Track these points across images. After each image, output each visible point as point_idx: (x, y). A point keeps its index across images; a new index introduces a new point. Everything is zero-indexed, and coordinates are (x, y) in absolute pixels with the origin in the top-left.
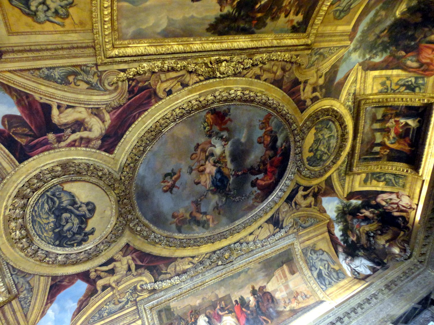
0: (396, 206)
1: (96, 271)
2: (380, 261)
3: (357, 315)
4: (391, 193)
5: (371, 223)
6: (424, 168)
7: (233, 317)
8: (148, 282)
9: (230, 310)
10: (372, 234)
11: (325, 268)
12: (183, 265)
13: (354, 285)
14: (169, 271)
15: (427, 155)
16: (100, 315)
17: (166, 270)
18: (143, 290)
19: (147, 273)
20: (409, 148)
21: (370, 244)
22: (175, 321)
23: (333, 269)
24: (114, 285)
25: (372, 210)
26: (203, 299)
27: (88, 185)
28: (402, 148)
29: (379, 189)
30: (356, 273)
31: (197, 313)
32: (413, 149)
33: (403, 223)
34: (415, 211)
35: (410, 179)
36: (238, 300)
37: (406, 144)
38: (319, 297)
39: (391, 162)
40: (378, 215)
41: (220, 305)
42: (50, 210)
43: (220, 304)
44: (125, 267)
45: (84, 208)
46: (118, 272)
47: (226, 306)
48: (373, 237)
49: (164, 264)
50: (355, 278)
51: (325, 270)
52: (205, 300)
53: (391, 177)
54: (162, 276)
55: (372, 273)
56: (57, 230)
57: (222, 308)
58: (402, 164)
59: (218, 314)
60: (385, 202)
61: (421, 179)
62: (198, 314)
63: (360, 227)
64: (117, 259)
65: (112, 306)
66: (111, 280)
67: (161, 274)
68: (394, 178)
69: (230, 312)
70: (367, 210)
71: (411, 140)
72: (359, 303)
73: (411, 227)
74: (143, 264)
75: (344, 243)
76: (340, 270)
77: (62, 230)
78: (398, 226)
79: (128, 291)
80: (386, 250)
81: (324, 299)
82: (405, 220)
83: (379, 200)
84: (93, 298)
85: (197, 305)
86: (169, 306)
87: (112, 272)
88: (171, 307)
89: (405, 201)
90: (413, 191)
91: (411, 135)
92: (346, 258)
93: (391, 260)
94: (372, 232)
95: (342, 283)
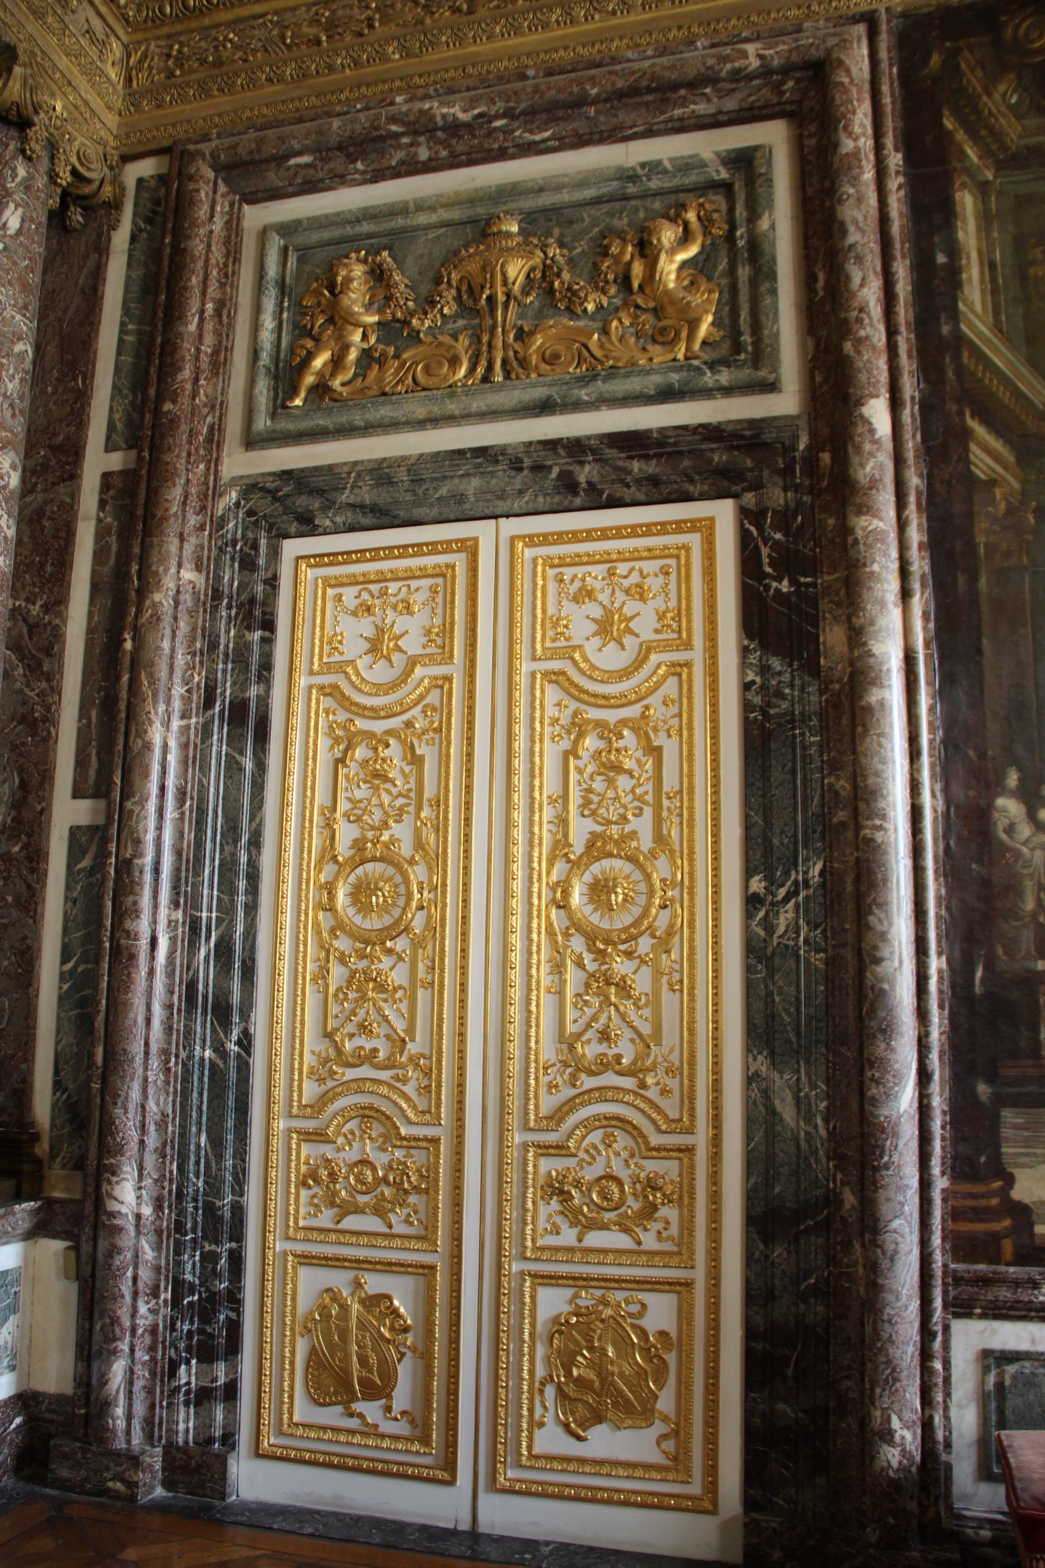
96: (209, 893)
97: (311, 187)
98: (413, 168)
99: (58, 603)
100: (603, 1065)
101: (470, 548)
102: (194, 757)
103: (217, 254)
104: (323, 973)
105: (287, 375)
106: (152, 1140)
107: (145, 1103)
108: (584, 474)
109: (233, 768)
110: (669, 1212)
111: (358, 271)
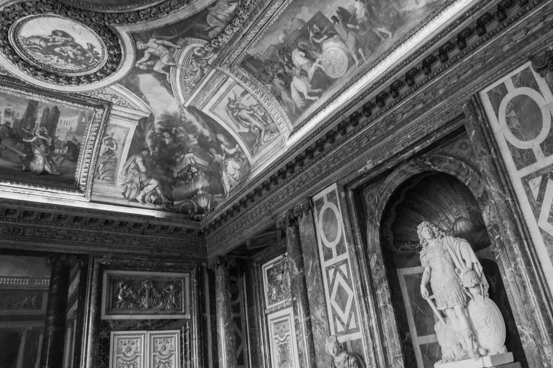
1: (140, 64)
7: (335, 41)
8: (202, 46)
9: (330, 32)
12: (224, 10)
14: (211, 25)
16: (189, 86)
17: (209, 26)
18: (205, 54)
19: (189, 39)
22: (266, 67)
24: (171, 64)
26: (285, 32)
27: (31, 22)
31: (287, 51)
36: (337, 15)
41: (313, 32)
42: (43, 54)
43: (312, 28)
44: (161, 48)
45: (57, 38)
46: (160, 55)
47: (322, 29)
49: (199, 22)
52: (288, 33)
54: (211, 34)
56: (70, 60)
57: (317, 33)
59: (314, 42)
62: (289, 52)
64: (143, 48)
65: (192, 77)
66: (165, 60)
67: (207, 33)
69: (331, 36)
74: (177, 36)
77: (71, 58)
79: (192, 62)
84: (168, 79)
85: (282, 41)
86: (249, 55)
87: (154, 58)
88: (252, 55)
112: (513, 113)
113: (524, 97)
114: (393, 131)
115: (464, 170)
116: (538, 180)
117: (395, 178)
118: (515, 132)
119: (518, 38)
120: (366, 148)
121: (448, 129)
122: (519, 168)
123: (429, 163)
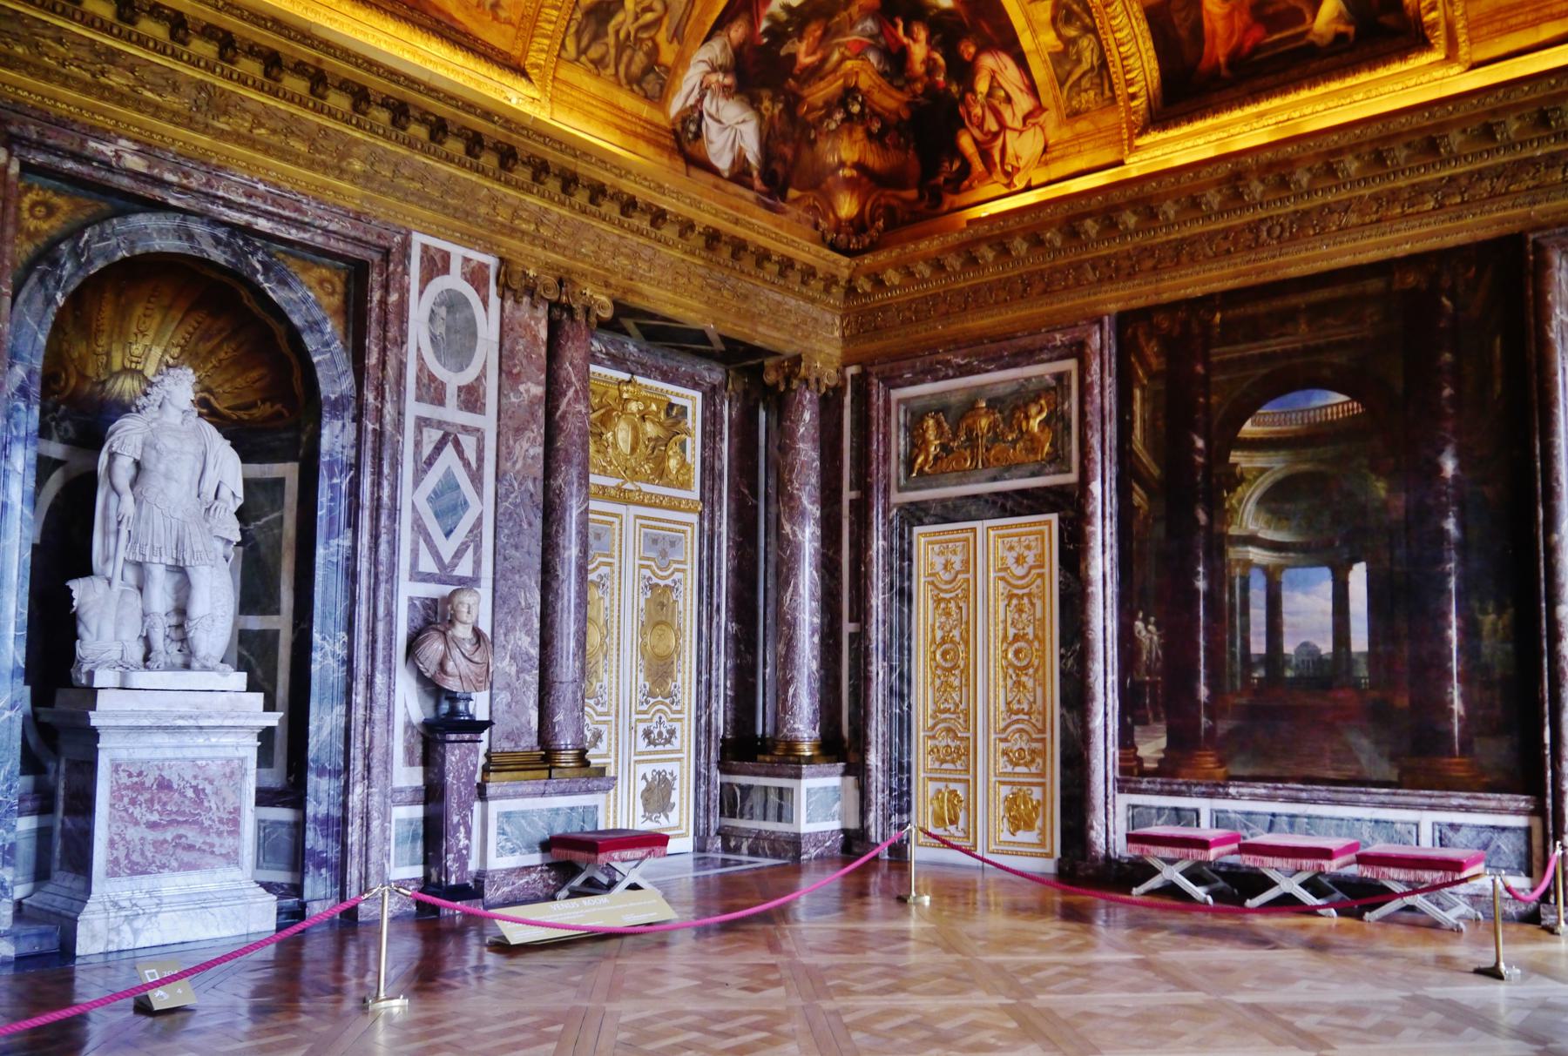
0: (994, 127)
2: (781, 179)
3: (563, 196)
4: (1032, 89)
5: (891, 83)
6: (1165, 141)
10: (856, 109)
11: (637, 18)
13: (649, 141)
15: (1215, 128)
20: (1222, 60)
21: (821, 120)
23: (656, 48)
25: (941, 61)
28: (1214, 32)
29: (1026, 41)
30: (693, 128)
32: (1224, 72)
33: (947, 181)
34: (1005, 191)
35: (1110, 119)
37: (1235, 39)
38: (526, 53)
39: (1144, 26)
40: (931, 89)
48: (849, 117)
50: (674, 132)
51: (630, 19)
53: (1089, 58)
55: (726, 174)
58: (1154, 65)
60: (991, 87)
61: (1122, 152)
63: (857, 56)
68: (1092, 68)
70: (929, 42)
71: (1257, 49)
72: (603, 185)
73: (946, 207)
75: (767, 32)
76: (668, 70)
78: (930, 167)
80: (830, 180)
81: (533, 72)
82: (962, 178)
83: (988, 62)
89: (1023, 146)
90: (1071, 150)
91: (1276, 37)
92: (724, 69)
93: (809, 208)
94: (862, 105)
95: (627, 101)
96: (895, 656)
97: (913, 383)
98: (946, 377)
99: (839, 551)
100: (1018, 712)
101: (974, 530)
102: (888, 608)
103: (882, 414)
104: (933, 682)
105: (910, 463)
106: (880, 740)
107: (877, 728)
108: (1009, 504)
109: (901, 612)
110: (1039, 760)
111: (931, 422)
112: (443, 311)
113: (466, 303)
114: (221, 135)
115: (322, 332)
116: (437, 435)
117: (160, 231)
118: (434, 339)
119: (503, 216)
120: (120, 98)
121: (341, 245)
122: (419, 399)
123: (258, 266)
